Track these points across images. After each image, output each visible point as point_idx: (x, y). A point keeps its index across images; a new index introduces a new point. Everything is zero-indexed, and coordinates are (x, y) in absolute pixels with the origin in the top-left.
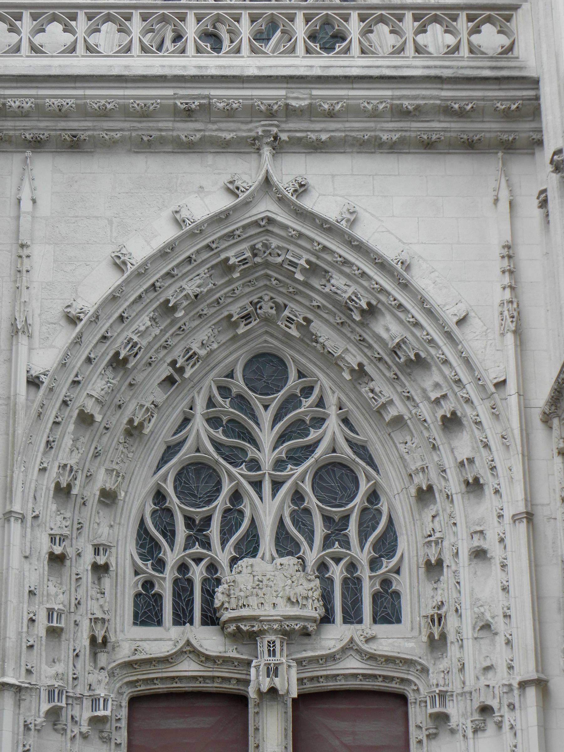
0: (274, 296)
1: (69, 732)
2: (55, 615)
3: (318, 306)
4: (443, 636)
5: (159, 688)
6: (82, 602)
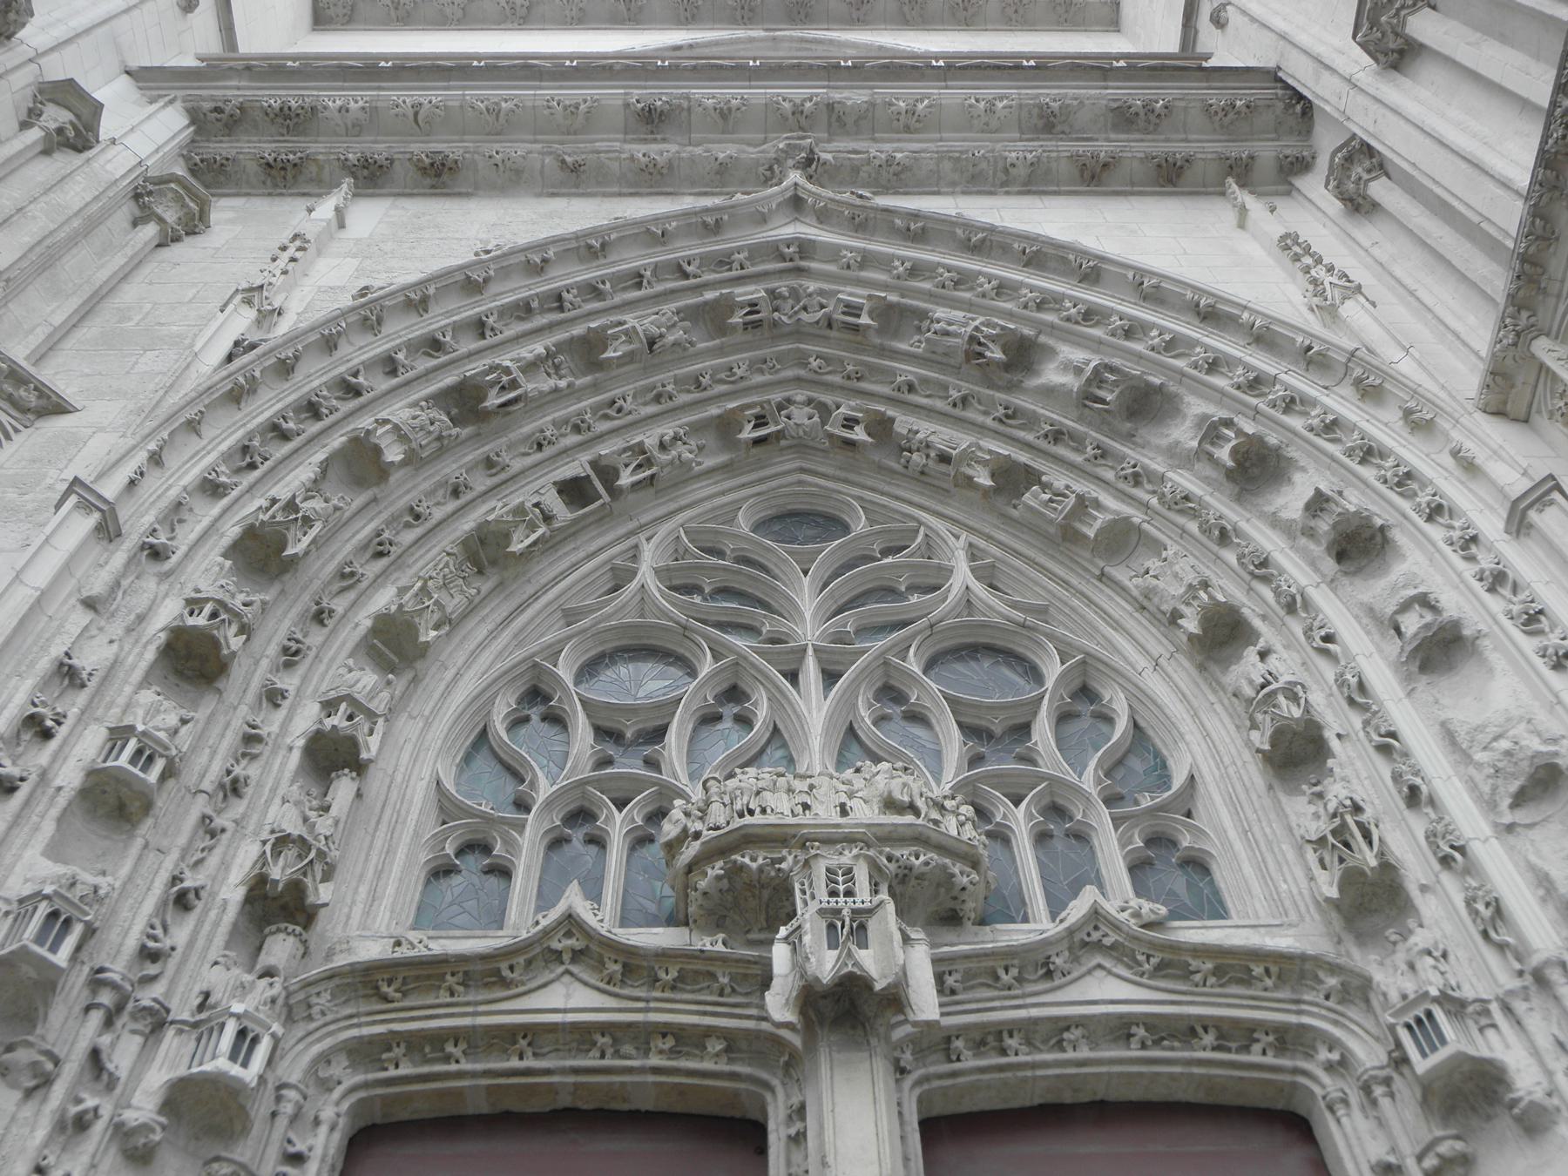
0: (815, 395)
1: (58, 1091)
2: (132, 745)
3: (911, 388)
4: (1388, 868)
5: (460, 1075)
6: (249, 791)
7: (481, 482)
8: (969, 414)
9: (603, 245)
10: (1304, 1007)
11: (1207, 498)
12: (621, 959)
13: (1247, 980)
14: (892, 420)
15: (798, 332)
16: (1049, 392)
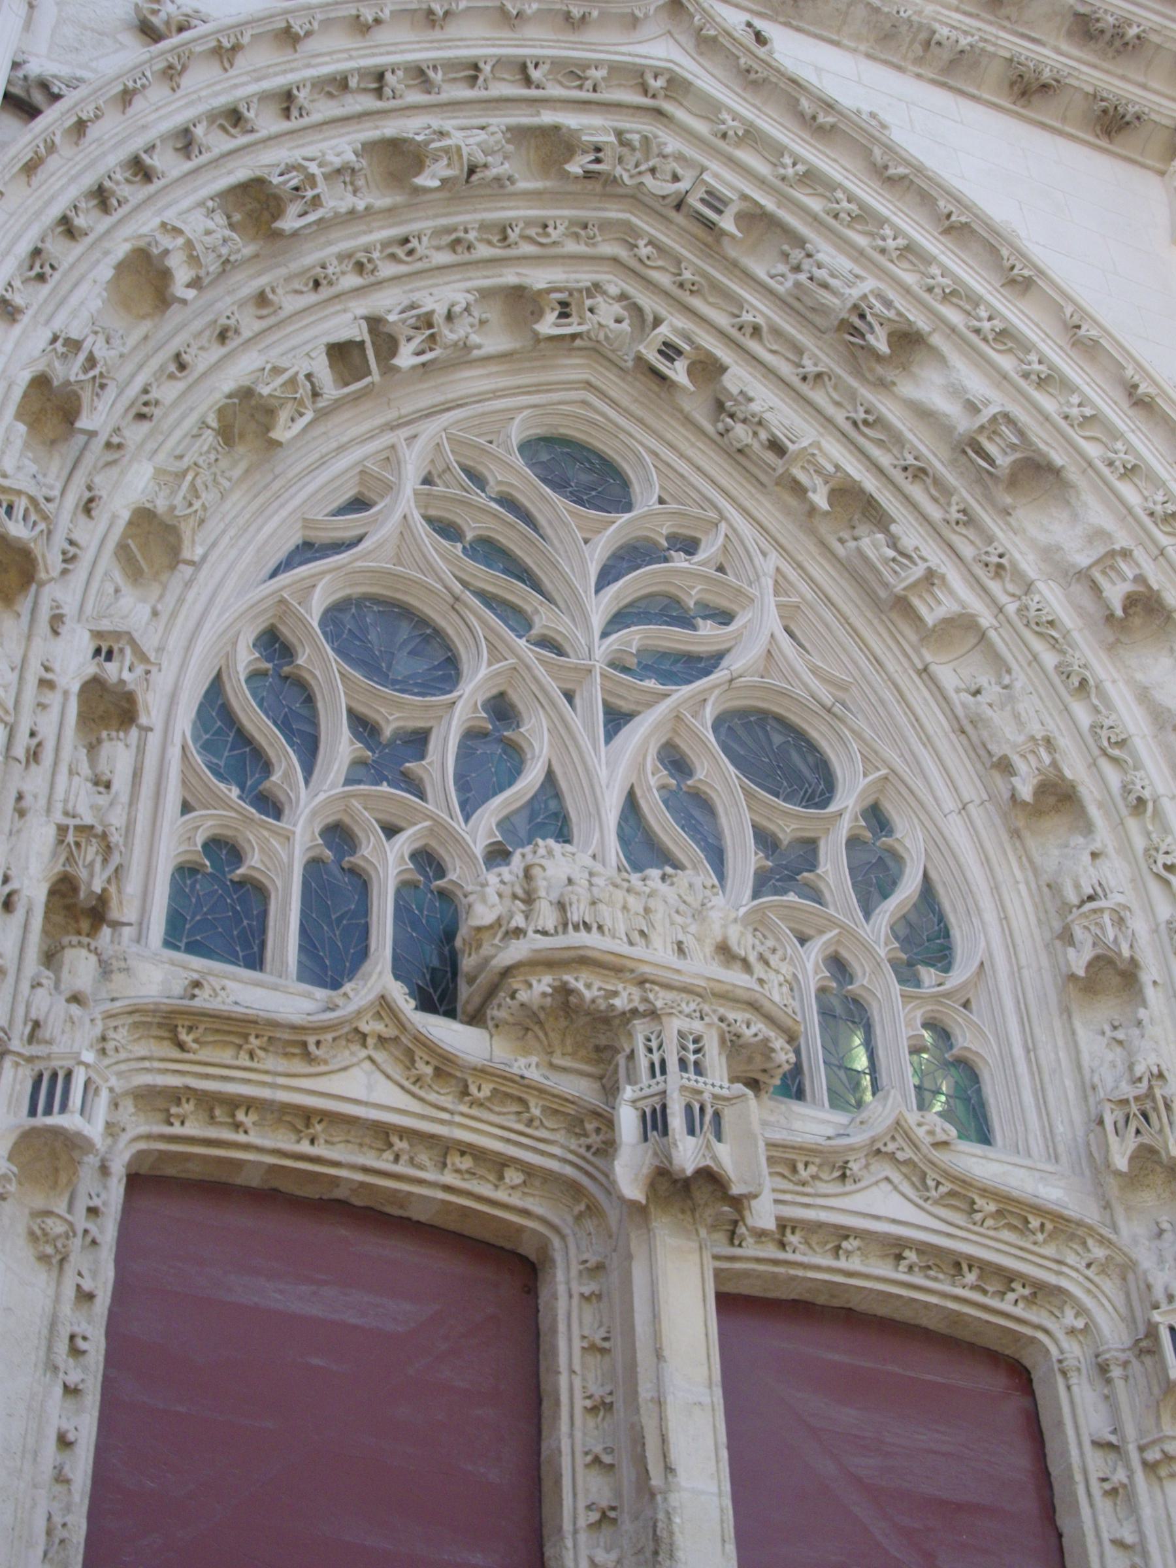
3: (756, 331)
5: (247, 1147)
7: (249, 324)
8: (818, 397)
9: (447, 13)
10: (1065, 1269)
11: (1076, 635)
12: (434, 1062)
13: (1023, 1228)
14: (723, 369)
15: (637, 198)
16: (924, 414)
